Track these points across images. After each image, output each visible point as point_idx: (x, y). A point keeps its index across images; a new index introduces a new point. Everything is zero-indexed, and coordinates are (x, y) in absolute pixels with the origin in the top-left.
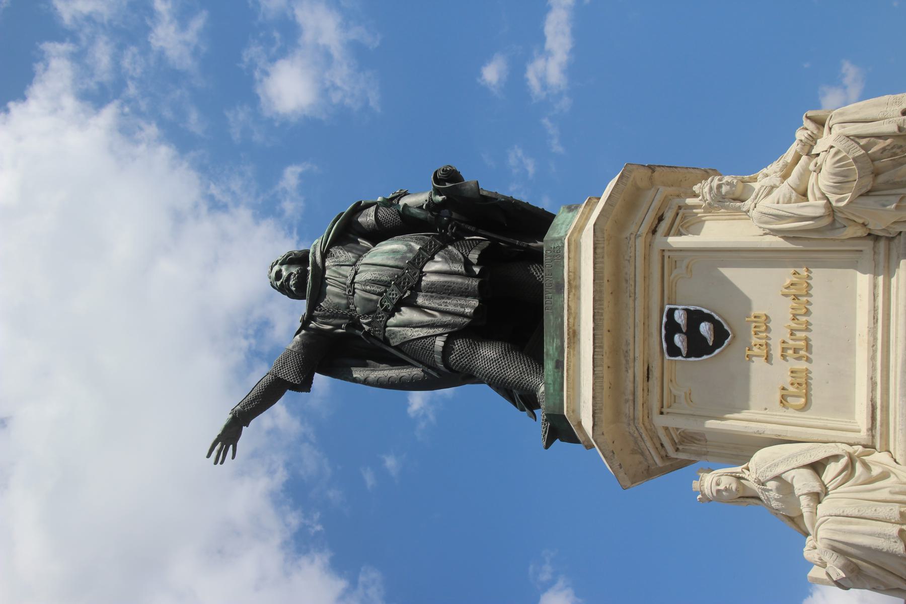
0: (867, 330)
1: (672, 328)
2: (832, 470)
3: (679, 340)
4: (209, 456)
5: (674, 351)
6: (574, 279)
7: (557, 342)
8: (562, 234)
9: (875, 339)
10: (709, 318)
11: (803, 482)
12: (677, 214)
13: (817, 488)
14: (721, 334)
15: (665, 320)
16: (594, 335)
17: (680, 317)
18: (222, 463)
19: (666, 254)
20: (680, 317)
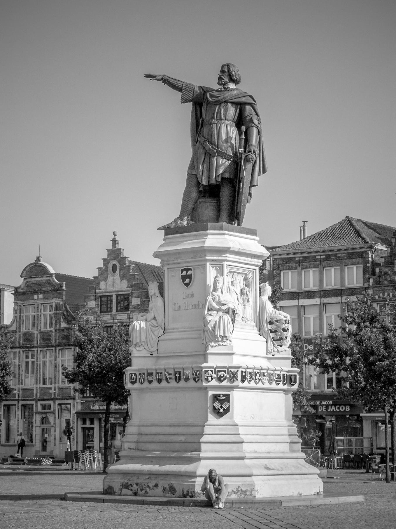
1: (187, 270)
5: (182, 271)
10: (190, 281)
11: (150, 316)
13: (148, 320)
14: (187, 285)
17: (190, 273)
20: (190, 273)
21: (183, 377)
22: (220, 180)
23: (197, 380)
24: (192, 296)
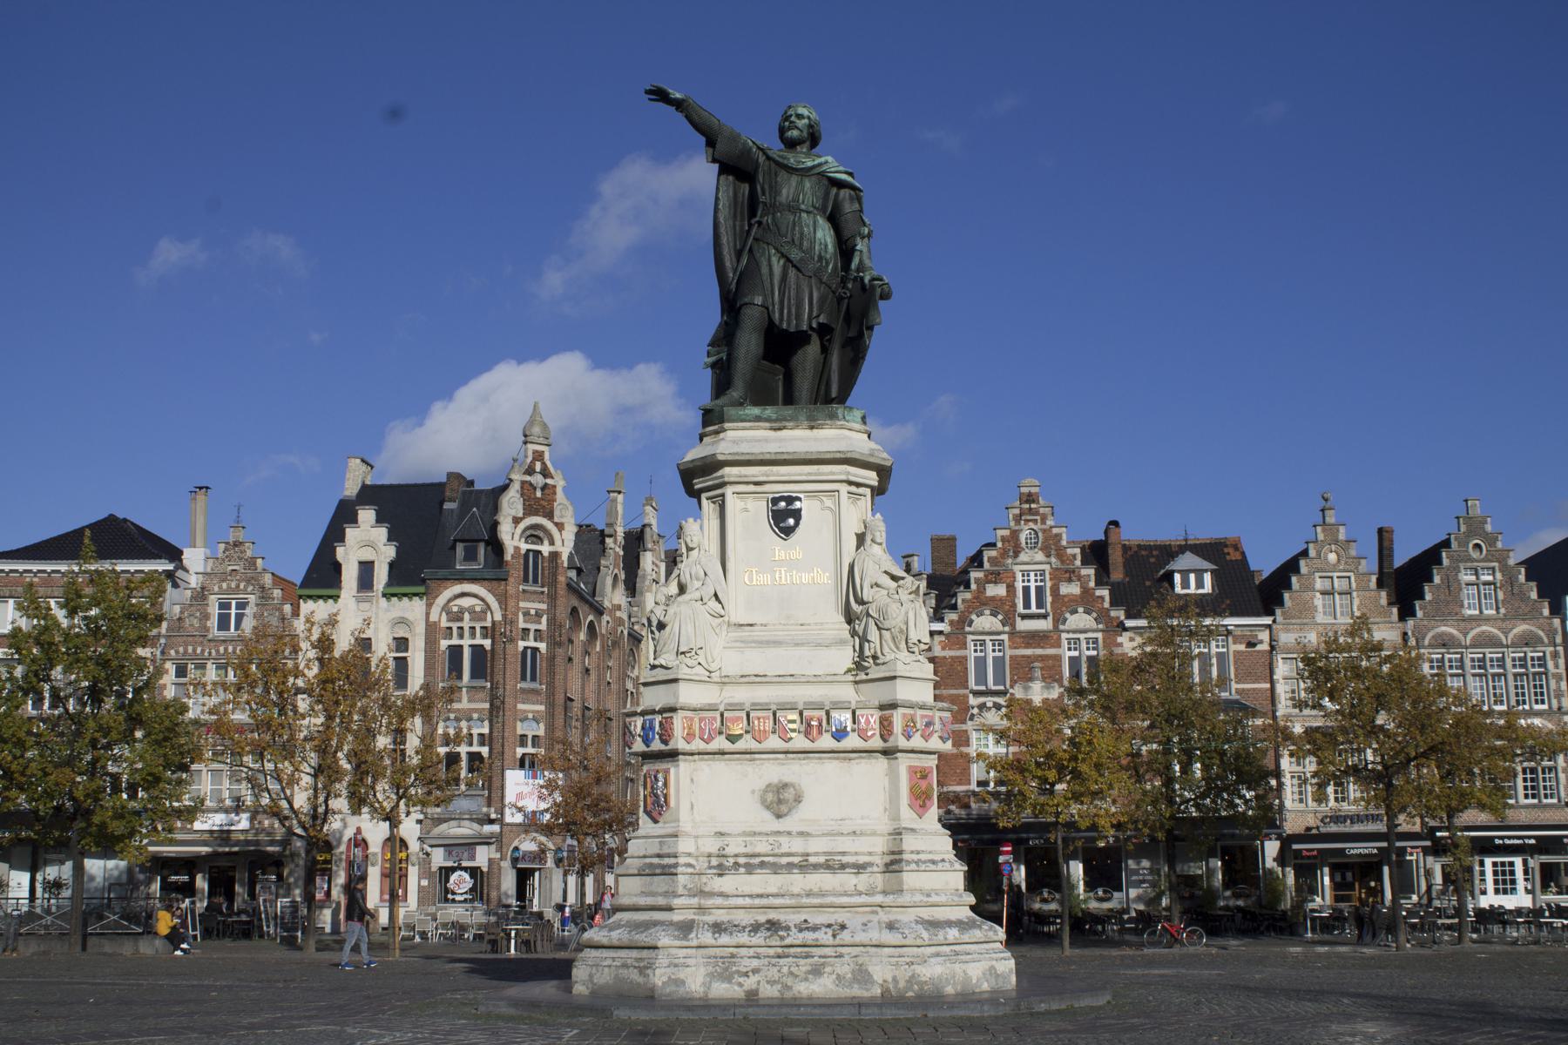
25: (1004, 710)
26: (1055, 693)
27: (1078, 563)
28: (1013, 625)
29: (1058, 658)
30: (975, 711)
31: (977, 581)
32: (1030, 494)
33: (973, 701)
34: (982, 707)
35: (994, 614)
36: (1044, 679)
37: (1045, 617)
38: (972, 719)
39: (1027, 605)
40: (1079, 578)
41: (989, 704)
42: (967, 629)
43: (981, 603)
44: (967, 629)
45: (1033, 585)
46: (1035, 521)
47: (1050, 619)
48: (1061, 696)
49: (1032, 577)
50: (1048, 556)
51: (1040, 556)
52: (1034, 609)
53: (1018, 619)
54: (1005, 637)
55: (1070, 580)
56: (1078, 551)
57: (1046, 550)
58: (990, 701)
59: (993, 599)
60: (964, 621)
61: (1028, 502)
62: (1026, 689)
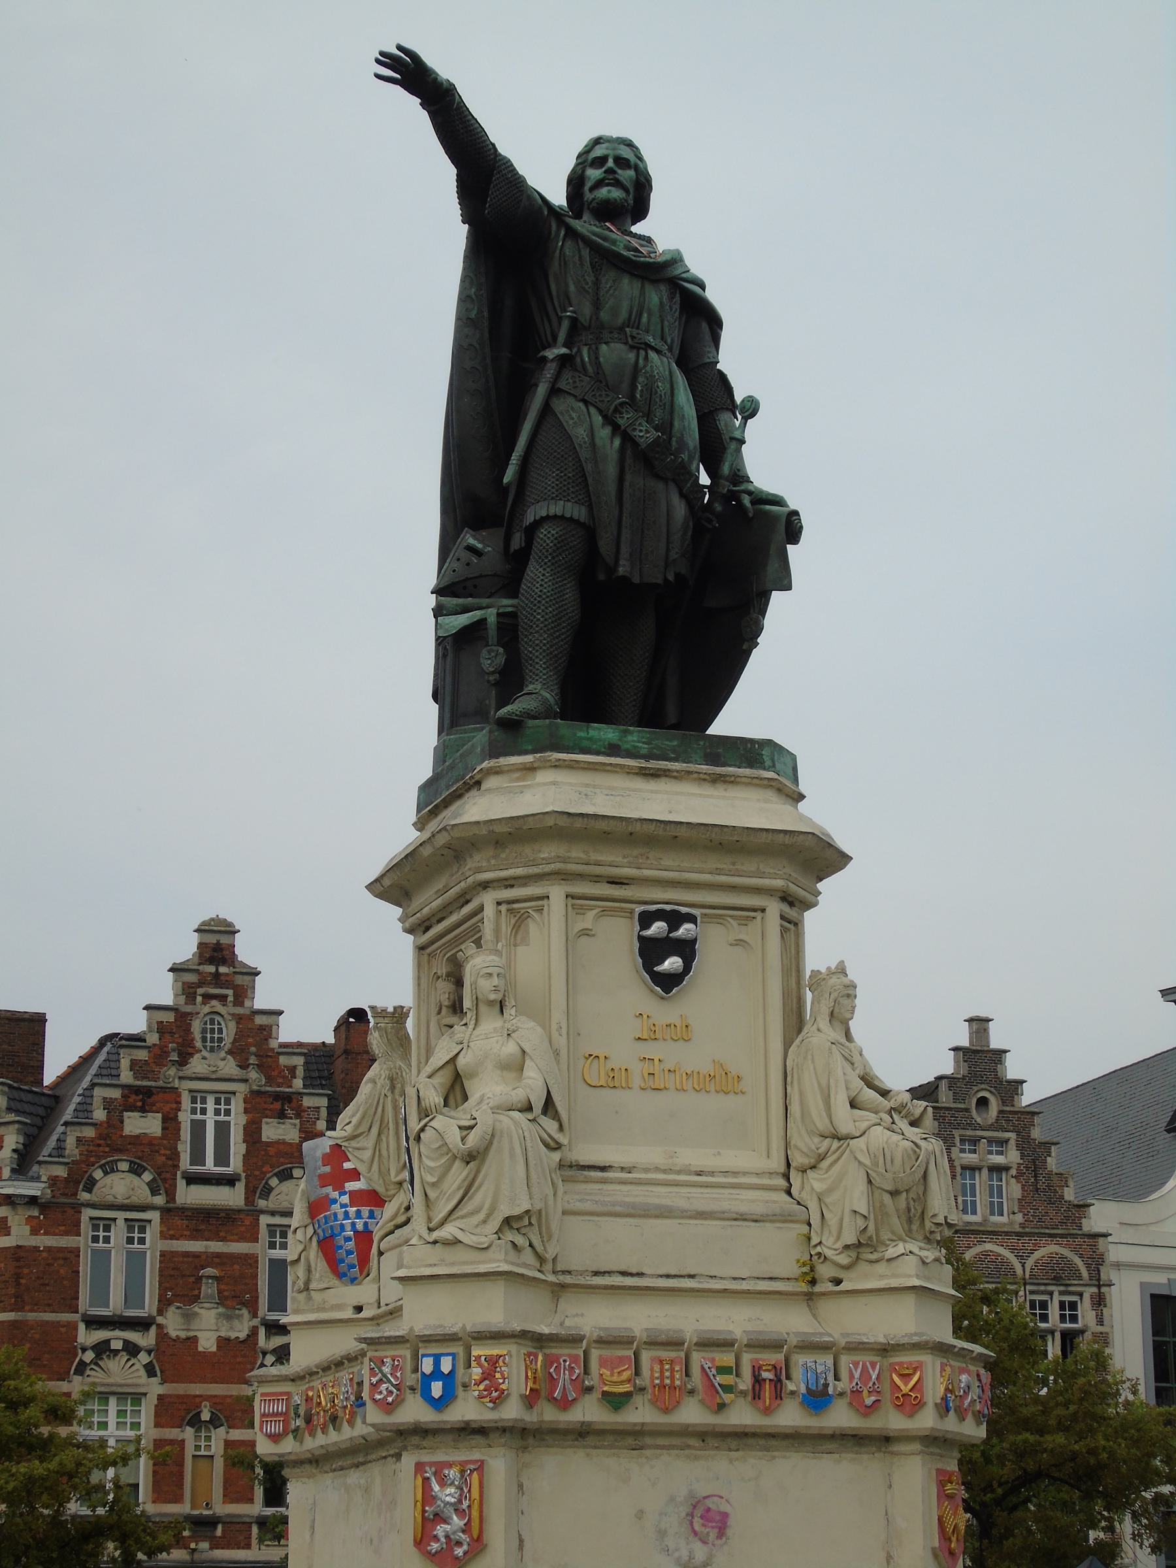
0: (687, 1163)
1: (675, 919)
2: (550, 1125)
3: (658, 928)
4: (399, 48)
5: (646, 919)
6: (725, 782)
7: (644, 749)
8: (778, 766)
9: (679, 1172)
10: (687, 968)
12: (790, 922)
14: (668, 983)
15: (684, 910)
16: (681, 823)
17: (685, 930)
18: (378, 61)
19: (759, 915)
20: (685, 930)
21: (797, 1384)
22: (671, 578)
23: (869, 1401)
24: (683, 1033)
25: (144, 1358)
26: (240, 1330)
27: (298, 1083)
28: (171, 1195)
29: (250, 1261)
30: (89, 1356)
31: (108, 1104)
32: (218, 947)
33: (86, 1337)
34: (102, 1349)
35: (136, 1170)
36: (222, 1300)
37: (230, 1181)
38: (82, 1368)
39: (198, 1156)
40: (299, 1112)
41: (116, 1345)
42: (84, 1196)
43: (110, 1146)
44: (84, 1196)
45: (210, 1120)
46: (223, 998)
47: (240, 1187)
48: (254, 1332)
49: (210, 1106)
50: (243, 1066)
51: (229, 1067)
52: (210, 1165)
53: (181, 1183)
54: (155, 1216)
55: (281, 1116)
56: (299, 1061)
57: (238, 1052)
58: (117, 1338)
59: (136, 1140)
60: (79, 1179)
61: (211, 961)
62: (189, 1317)
